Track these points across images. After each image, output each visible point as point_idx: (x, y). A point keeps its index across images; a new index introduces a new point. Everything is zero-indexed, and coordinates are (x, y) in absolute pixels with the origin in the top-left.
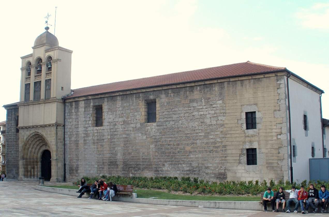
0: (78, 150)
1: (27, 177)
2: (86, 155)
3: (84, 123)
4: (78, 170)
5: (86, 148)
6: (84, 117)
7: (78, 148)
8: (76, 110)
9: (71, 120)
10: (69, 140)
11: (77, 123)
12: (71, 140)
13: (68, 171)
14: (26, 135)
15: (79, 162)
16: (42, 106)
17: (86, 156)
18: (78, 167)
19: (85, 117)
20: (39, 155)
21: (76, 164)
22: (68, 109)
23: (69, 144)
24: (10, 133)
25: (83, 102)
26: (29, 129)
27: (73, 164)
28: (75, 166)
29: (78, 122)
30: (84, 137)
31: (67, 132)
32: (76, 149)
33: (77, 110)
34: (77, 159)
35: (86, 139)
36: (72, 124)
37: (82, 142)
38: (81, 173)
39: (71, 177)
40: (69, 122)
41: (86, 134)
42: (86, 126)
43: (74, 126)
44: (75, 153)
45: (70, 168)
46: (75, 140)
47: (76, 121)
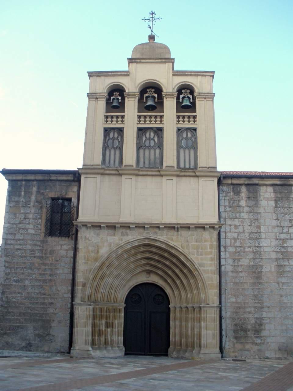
0: (262, 287)
1: (99, 348)
2: (284, 298)
3: (276, 230)
4: (261, 330)
5: (283, 283)
6: (275, 218)
7: (261, 281)
8: (251, 203)
9: (236, 222)
10: (231, 263)
11: (254, 229)
12: (240, 263)
13: (230, 333)
14: (106, 244)
15: (264, 314)
17: (285, 299)
18: (261, 325)
19: (277, 219)
20: (122, 294)
21: (256, 316)
22: (227, 198)
23: (232, 272)
24: (18, 236)
25: (270, 189)
26: (119, 232)
27: (246, 316)
28: (253, 321)
29: (259, 227)
30: (277, 259)
32: (253, 283)
33: (254, 203)
35: (282, 263)
36: (241, 229)
37: (273, 270)
38: (270, 336)
39: (239, 346)
40: (230, 225)
41: (282, 253)
42: (283, 236)
43: (247, 235)
44: (252, 293)
45: (236, 325)
46: (252, 264)
47: (253, 224)
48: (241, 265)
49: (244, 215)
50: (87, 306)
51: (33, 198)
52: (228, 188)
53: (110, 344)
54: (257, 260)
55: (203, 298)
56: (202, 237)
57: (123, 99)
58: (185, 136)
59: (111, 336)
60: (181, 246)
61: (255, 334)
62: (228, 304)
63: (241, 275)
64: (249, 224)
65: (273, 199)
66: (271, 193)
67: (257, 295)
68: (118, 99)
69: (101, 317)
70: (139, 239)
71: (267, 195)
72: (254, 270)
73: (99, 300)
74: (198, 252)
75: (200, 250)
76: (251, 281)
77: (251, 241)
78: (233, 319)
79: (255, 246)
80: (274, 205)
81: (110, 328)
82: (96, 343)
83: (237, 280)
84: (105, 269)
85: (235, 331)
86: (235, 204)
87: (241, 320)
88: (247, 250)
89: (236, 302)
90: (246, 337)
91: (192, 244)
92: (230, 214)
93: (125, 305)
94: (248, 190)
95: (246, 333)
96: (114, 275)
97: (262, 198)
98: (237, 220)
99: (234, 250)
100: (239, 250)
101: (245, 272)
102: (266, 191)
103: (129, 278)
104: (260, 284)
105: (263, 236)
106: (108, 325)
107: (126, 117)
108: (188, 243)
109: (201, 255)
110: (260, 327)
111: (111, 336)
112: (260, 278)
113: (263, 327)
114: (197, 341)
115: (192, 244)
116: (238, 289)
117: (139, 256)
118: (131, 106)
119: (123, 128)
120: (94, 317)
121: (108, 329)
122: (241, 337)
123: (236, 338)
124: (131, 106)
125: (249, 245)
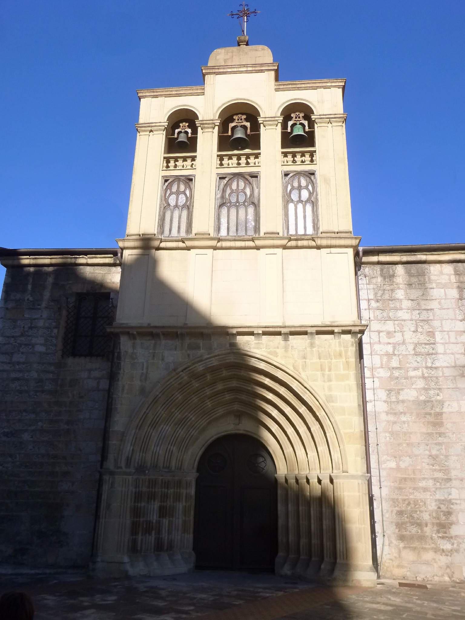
0: (445, 440)
4: (451, 524)
7: (442, 430)
8: (415, 293)
9: (390, 326)
10: (384, 398)
11: (423, 338)
12: (401, 398)
13: (391, 530)
15: (454, 491)
16: (269, 260)
18: (449, 513)
21: (438, 497)
22: (371, 286)
23: (387, 413)
24: (16, 358)
25: (449, 269)
27: (419, 495)
28: (432, 506)
29: (431, 334)
31: (372, 369)
34: (440, 475)
36: (398, 337)
39: (409, 556)
40: (379, 332)
44: (427, 452)
45: (400, 513)
46: (422, 398)
47: (420, 330)
48: (403, 401)
49: (403, 315)
50: (125, 477)
51: (47, 294)
52: (373, 270)
53: (165, 548)
54: (432, 392)
55: (336, 460)
56: (330, 350)
57: (195, 132)
58: (296, 184)
59: (169, 533)
60: (293, 366)
61: (438, 532)
62: (383, 473)
63: (403, 418)
64: (413, 329)
65: (455, 285)
66: (449, 275)
67: (437, 456)
68: (186, 133)
69: (151, 497)
70: (218, 355)
71: (444, 279)
72: (428, 410)
73: (149, 464)
74: (323, 375)
75: (327, 372)
76: (424, 430)
77: (419, 359)
78: (395, 501)
79: (427, 367)
80: (457, 296)
81: (167, 518)
82: (139, 549)
83: (397, 428)
84: (159, 408)
85: (399, 526)
86: (387, 296)
87: (409, 504)
88: (412, 373)
89: (398, 469)
90: (422, 538)
91: (311, 361)
92: (378, 313)
93: (198, 474)
94: (409, 274)
95: (422, 530)
96: (176, 419)
97: (434, 285)
98: (390, 323)
99: (388, 374)
100: (396, 373)
101: (411, 414)
102: (441, 273)
103: (204, 424)
104: (440, 434)
105: (440, 349)
106: (163, 512)
107: (198, 159)
108: (304, 360)
109: (330, 380)
110: (448, 519)
111: (169, 533)
112: (441, 424)
113: (453, 518)
114: (328, 544)
115: (311, 361)
116: (399, 445)
117: (220, 387)
118: (207, 141)
119: (194, 176)
120: (138, 497)
121: (164, 520)
122: (412, 538)
123: (402, 538)
124: (207, 141)
125: (415, 364)
